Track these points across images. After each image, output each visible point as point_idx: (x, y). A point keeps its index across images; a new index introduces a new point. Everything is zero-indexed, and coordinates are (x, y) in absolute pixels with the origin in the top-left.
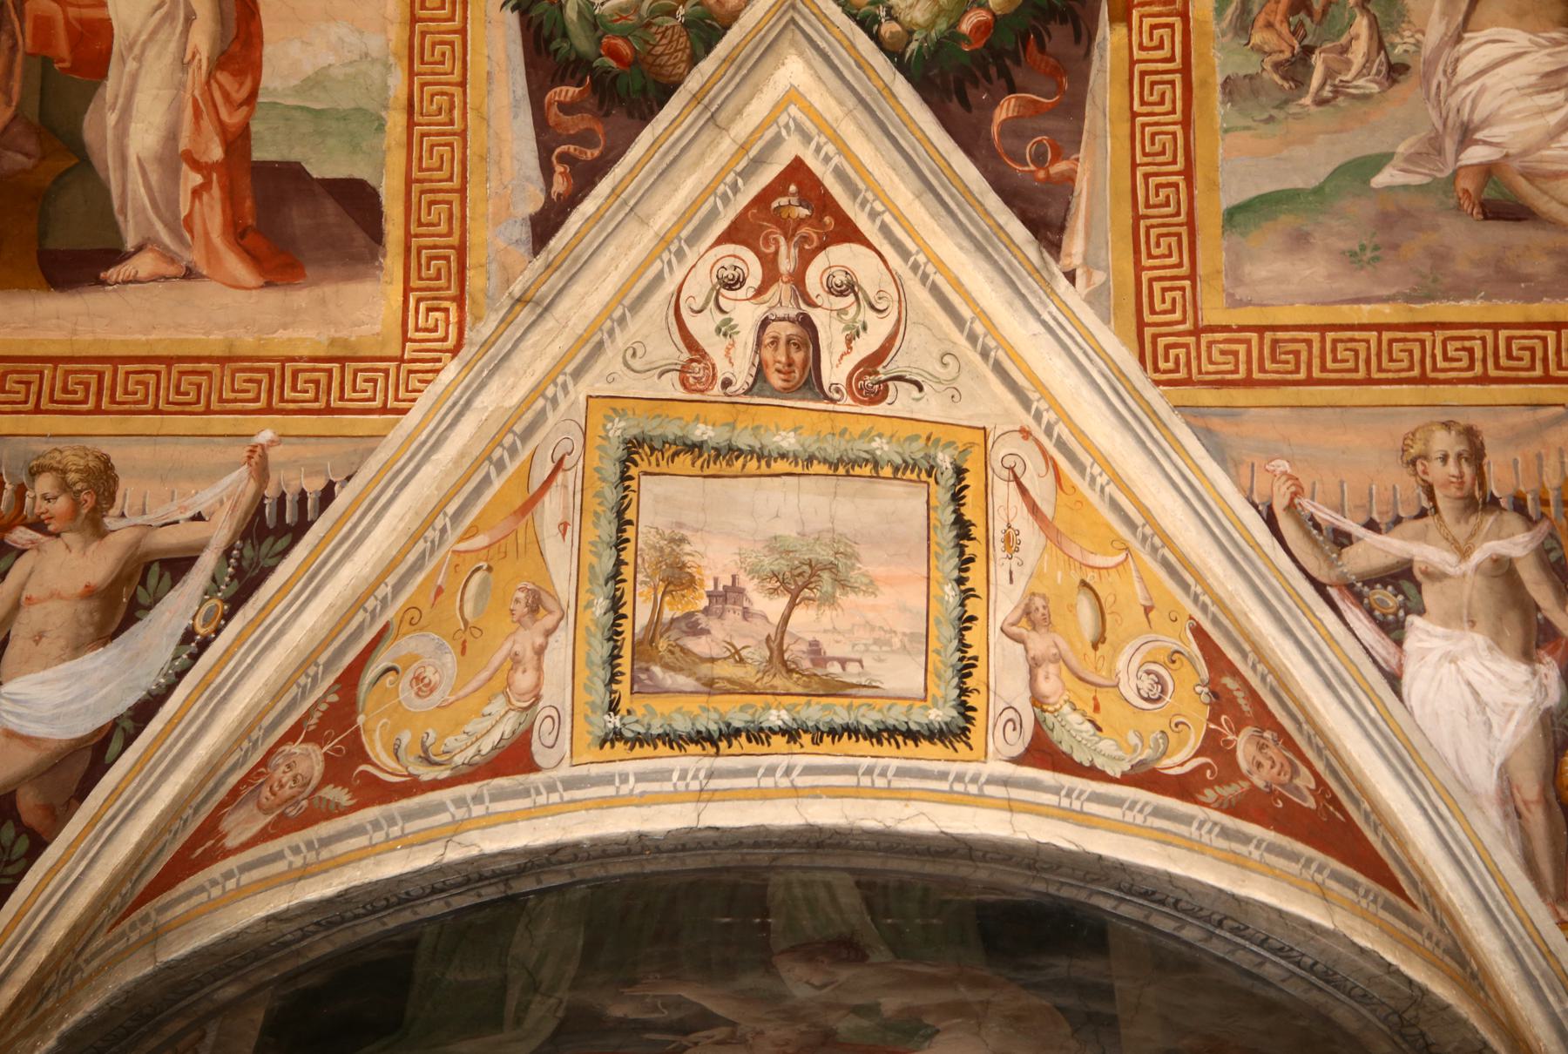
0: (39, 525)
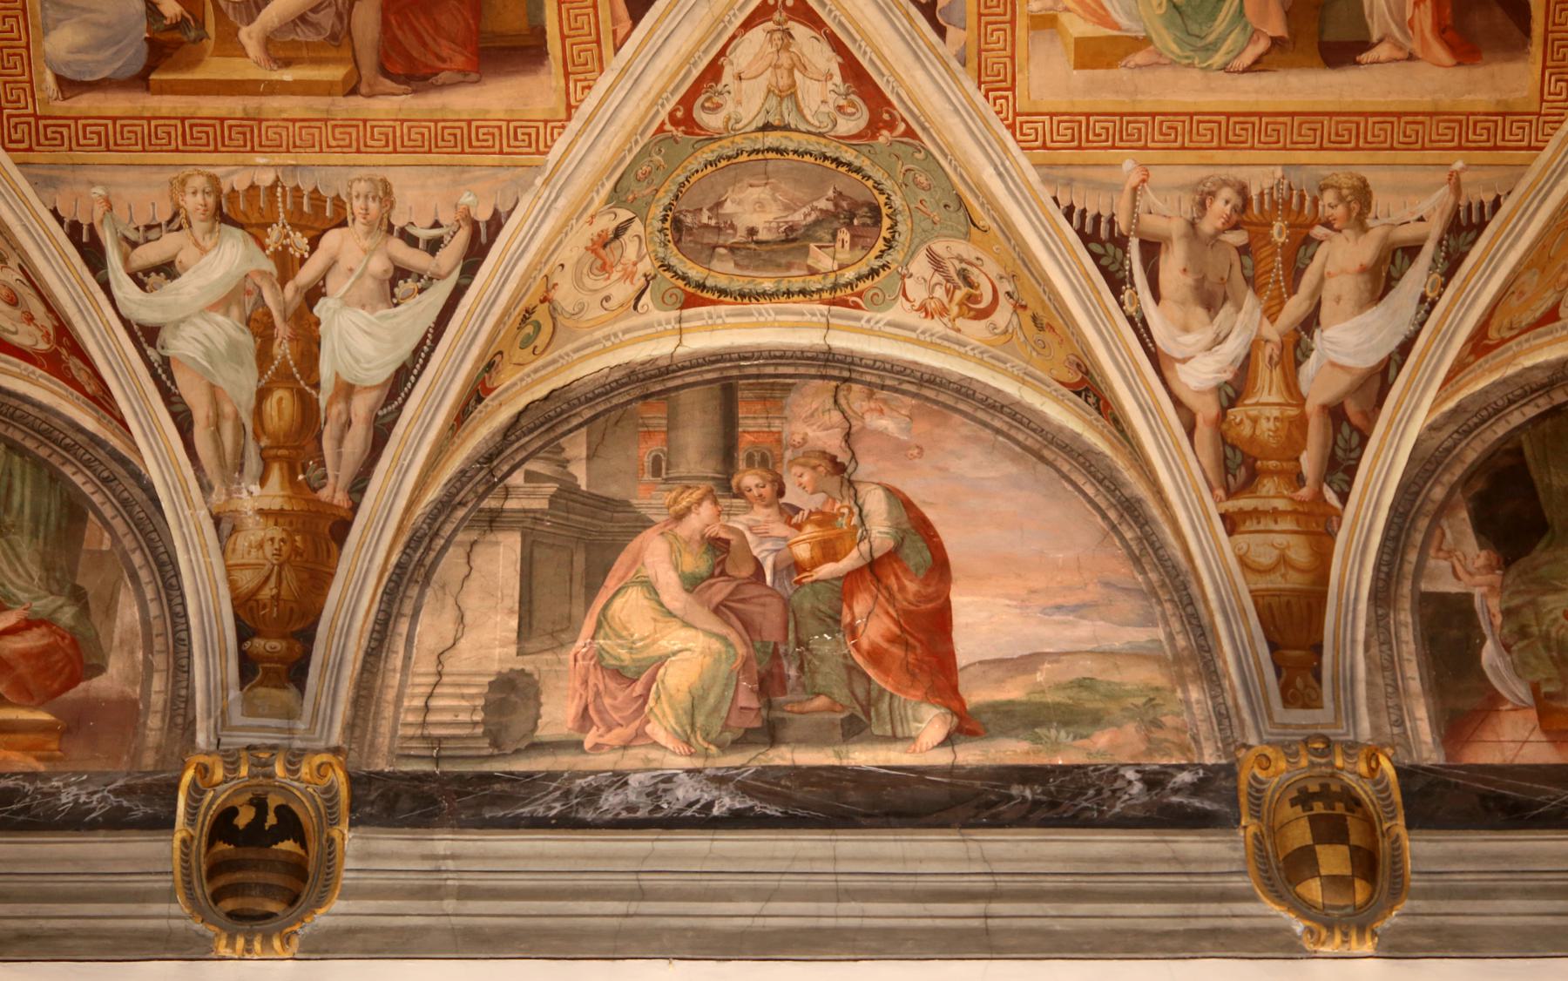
0: (1328, 224)
